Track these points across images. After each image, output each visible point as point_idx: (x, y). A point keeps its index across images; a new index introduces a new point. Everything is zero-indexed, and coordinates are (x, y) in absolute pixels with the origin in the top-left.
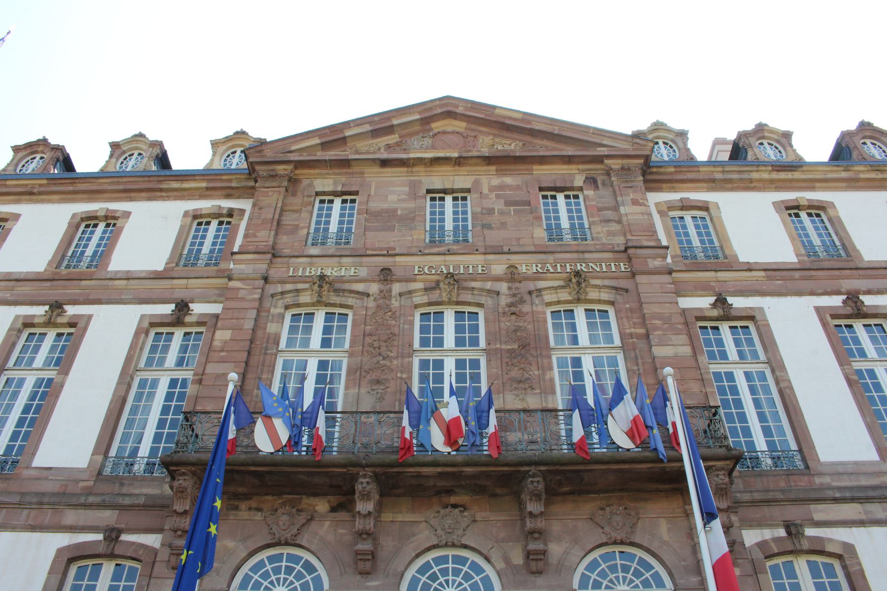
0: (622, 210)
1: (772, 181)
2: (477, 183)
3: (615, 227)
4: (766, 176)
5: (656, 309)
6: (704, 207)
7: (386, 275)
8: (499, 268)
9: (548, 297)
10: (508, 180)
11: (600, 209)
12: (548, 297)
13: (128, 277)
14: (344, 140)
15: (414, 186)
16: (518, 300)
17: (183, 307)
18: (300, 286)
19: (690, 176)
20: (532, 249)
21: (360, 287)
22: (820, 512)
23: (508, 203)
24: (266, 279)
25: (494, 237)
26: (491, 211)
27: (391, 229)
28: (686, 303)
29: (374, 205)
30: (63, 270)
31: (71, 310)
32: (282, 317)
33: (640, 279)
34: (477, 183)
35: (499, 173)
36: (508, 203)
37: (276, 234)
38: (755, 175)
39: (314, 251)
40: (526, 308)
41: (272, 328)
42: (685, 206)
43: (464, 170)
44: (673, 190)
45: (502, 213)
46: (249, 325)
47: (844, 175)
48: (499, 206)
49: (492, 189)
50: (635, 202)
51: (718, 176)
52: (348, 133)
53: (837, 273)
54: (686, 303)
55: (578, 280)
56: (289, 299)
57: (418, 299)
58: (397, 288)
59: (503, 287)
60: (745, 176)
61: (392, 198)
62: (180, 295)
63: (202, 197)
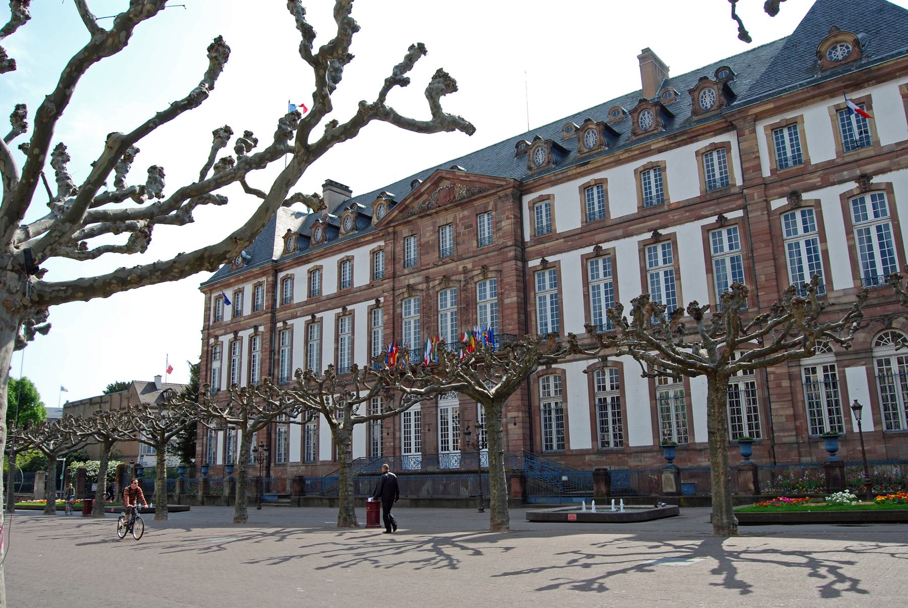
1: (579, 173)
2: (455, 217)
4: (574, 172)
6: (548, 197)
7: (427, 279)
8: (461, 268)
9: (476, 279)
10: (466, 213)
12: (476, 279)
14: (407, 207)
15: (434, 224)
16: (467, 282)
17: (378, 301)
18: (405, 290)
19: (541, 182)
20: (471, 254)
21: (420, 287)
23: (466, 228)
24: (393, 290)
27: (428, 253)
29: (423, 240)
30: (343, 289)
32: (401, 305)
33: (505, 264)
34: (455, 217)
35: (463, 210)
36: (466, 228)
37: (394, 264)
38: (570, 173)
39: (406, 271)
40: (469, 286)
41: (398, 310)
42: (542, 199)
43: (449, 212)
44: (535, 191)
45: (464, 234)
46: (391, 312)
47: (612, 159)
49: (461, 219)
51: (553, 178)
52: (407, 203)
53: (594, 232)
55: (485, 269)
56: (401, 297)
57: (438, 289)
58: (431, 284)
59: (462, 277)
60: (565, 175)
61: (428, 234)
62: (376, 294)
63: (373, 242)
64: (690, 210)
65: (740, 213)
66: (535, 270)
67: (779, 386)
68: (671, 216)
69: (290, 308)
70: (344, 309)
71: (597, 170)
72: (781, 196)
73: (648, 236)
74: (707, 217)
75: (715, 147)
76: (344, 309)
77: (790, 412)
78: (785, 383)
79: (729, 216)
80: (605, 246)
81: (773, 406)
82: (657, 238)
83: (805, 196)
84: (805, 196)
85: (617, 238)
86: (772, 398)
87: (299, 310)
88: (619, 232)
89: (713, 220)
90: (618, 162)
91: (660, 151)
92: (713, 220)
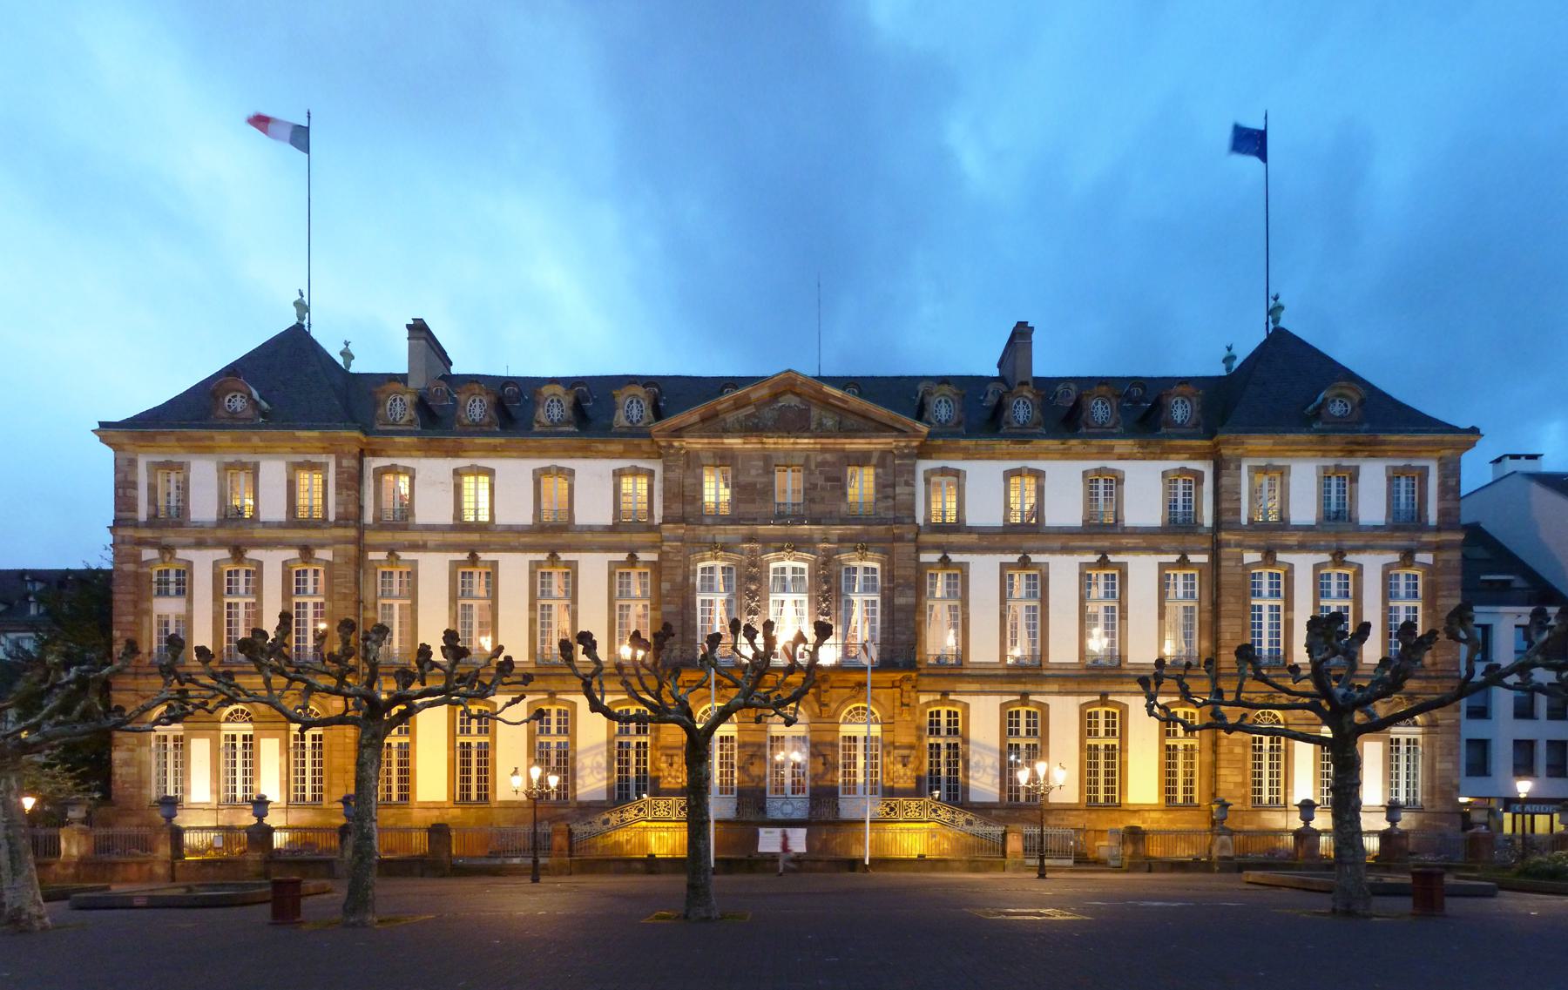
0: (898, 490)
3: (890, 502)
5: (902, 572)
11: (885, 486)
13: (590, 529)
22: (960, 687)
23: (828, 479)
25: (818, 508)
26: (814, 487)
27: (753, 501)
28: (926, 557)
31: (564, 556)
45: (823, 489)
48: (821, 482)
49: (819, 465)
50: (907, 484)
54: (926, 557)
61: (753, 472)
64: (1147, 540)
65: (1204, 558)
66: (931, 565)
67: (1231, 752)
68: (1125, 541)
69: (405, 528)
70: (553, 555)
71: (1035, 457)
72: (1257, 549)
73: (1093, 558)
74: (1167, 552)
75: (1183, 471)
76: (553, 555)
77: (1239, 779)
78: (1238, 750)
79: (1193, 558)
80: (1035, 558)
81: (1222, 772)
82: (1103, 563)
83: (1281, 557)
84: (1280, 557)
85: (1052, 551)
86: (1223, 763)
87: (433, 538)
88: (1057, 544)
89: (1174, 558)
90: (1066, 455)
91: (1121, 457)
92: (1174, 558)
